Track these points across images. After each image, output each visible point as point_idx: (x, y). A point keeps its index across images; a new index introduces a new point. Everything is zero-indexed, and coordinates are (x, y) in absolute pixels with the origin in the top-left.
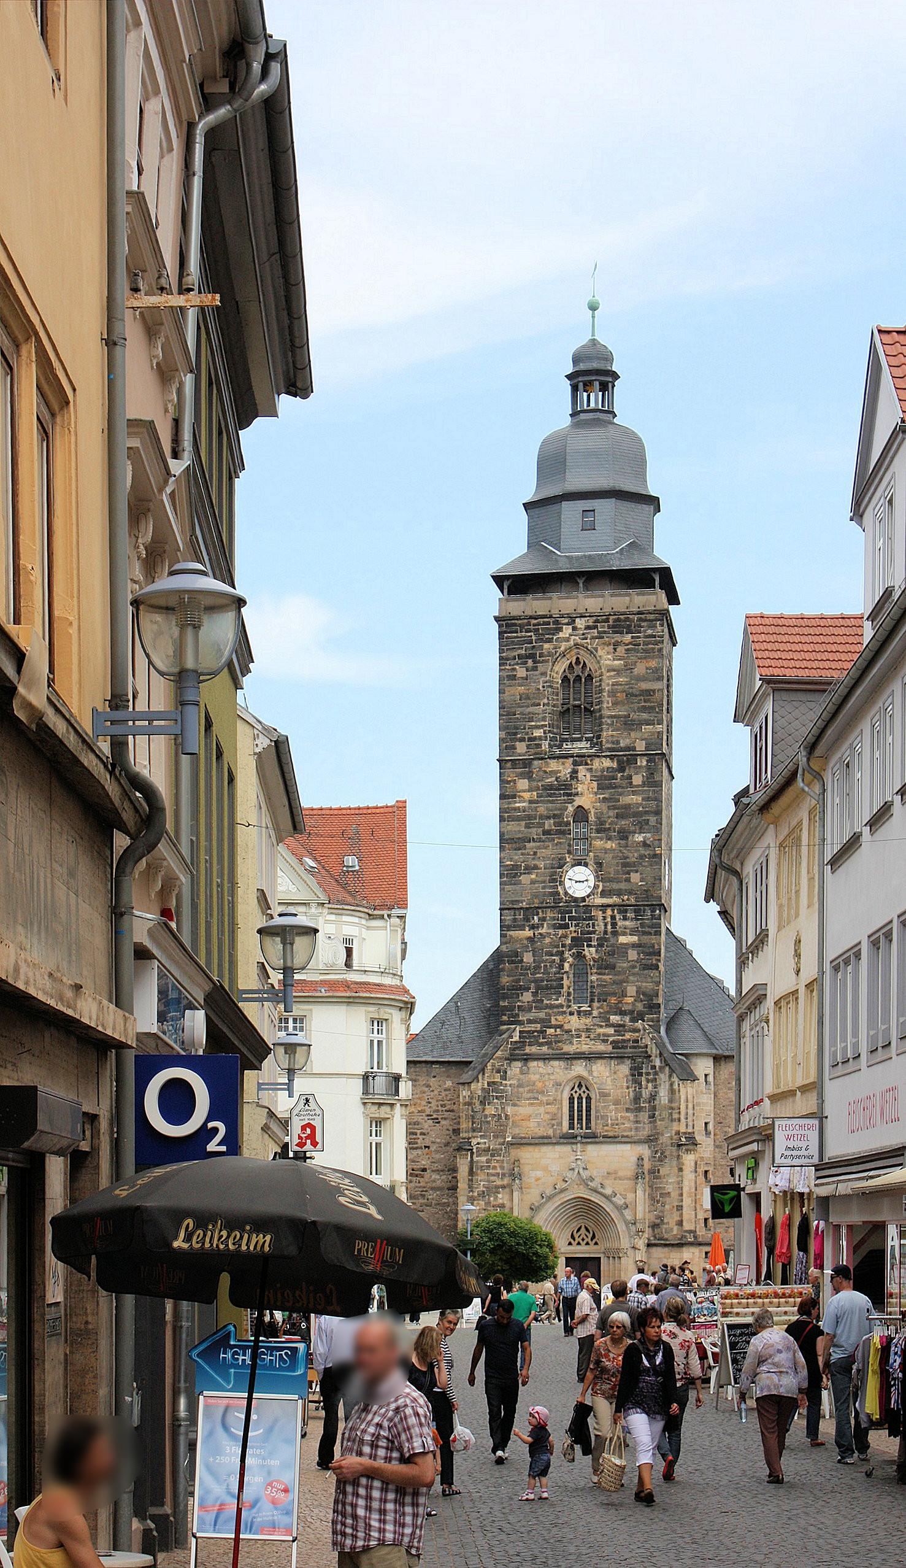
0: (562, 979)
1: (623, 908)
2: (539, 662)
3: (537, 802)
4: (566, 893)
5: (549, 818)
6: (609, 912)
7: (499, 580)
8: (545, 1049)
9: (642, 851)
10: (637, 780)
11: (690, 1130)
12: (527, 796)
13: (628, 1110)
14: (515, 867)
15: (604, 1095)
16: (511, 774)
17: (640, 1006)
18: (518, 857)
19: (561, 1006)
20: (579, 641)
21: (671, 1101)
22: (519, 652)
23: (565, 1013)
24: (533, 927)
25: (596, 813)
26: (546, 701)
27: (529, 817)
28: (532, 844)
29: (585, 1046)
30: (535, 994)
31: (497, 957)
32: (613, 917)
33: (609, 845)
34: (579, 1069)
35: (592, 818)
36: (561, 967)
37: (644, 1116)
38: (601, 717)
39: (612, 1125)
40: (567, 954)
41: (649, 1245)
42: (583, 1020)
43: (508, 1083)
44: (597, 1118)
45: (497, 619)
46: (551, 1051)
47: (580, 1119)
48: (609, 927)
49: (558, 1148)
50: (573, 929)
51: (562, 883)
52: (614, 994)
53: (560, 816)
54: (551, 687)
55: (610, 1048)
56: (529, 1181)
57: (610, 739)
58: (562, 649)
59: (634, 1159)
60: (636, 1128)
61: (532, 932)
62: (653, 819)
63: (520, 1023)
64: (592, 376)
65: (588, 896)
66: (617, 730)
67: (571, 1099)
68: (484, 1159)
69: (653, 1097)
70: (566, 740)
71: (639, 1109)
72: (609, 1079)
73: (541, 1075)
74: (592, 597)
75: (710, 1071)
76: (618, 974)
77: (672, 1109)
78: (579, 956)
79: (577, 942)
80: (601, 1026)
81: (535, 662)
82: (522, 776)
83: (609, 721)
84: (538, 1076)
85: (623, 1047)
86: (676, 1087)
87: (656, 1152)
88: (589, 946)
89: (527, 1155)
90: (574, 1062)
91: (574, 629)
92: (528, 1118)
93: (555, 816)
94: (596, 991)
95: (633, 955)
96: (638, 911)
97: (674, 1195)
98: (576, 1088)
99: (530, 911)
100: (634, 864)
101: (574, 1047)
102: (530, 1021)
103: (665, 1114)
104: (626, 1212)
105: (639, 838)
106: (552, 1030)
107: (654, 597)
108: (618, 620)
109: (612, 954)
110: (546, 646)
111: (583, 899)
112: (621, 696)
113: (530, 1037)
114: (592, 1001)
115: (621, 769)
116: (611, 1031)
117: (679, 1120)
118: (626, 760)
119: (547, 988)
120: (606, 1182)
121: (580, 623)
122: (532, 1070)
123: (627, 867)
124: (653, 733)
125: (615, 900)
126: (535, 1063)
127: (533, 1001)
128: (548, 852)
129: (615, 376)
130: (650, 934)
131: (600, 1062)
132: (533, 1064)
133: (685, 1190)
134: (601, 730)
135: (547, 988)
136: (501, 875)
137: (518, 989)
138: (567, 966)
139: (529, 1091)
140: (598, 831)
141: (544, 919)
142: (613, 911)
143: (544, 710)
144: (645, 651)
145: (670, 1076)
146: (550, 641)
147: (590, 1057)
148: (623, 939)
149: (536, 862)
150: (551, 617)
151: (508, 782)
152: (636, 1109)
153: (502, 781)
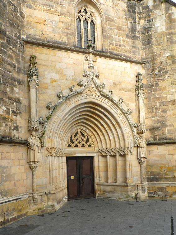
44: (103, 37)
56: (45, 81)
92: (44, 22)
98: (82, 13)
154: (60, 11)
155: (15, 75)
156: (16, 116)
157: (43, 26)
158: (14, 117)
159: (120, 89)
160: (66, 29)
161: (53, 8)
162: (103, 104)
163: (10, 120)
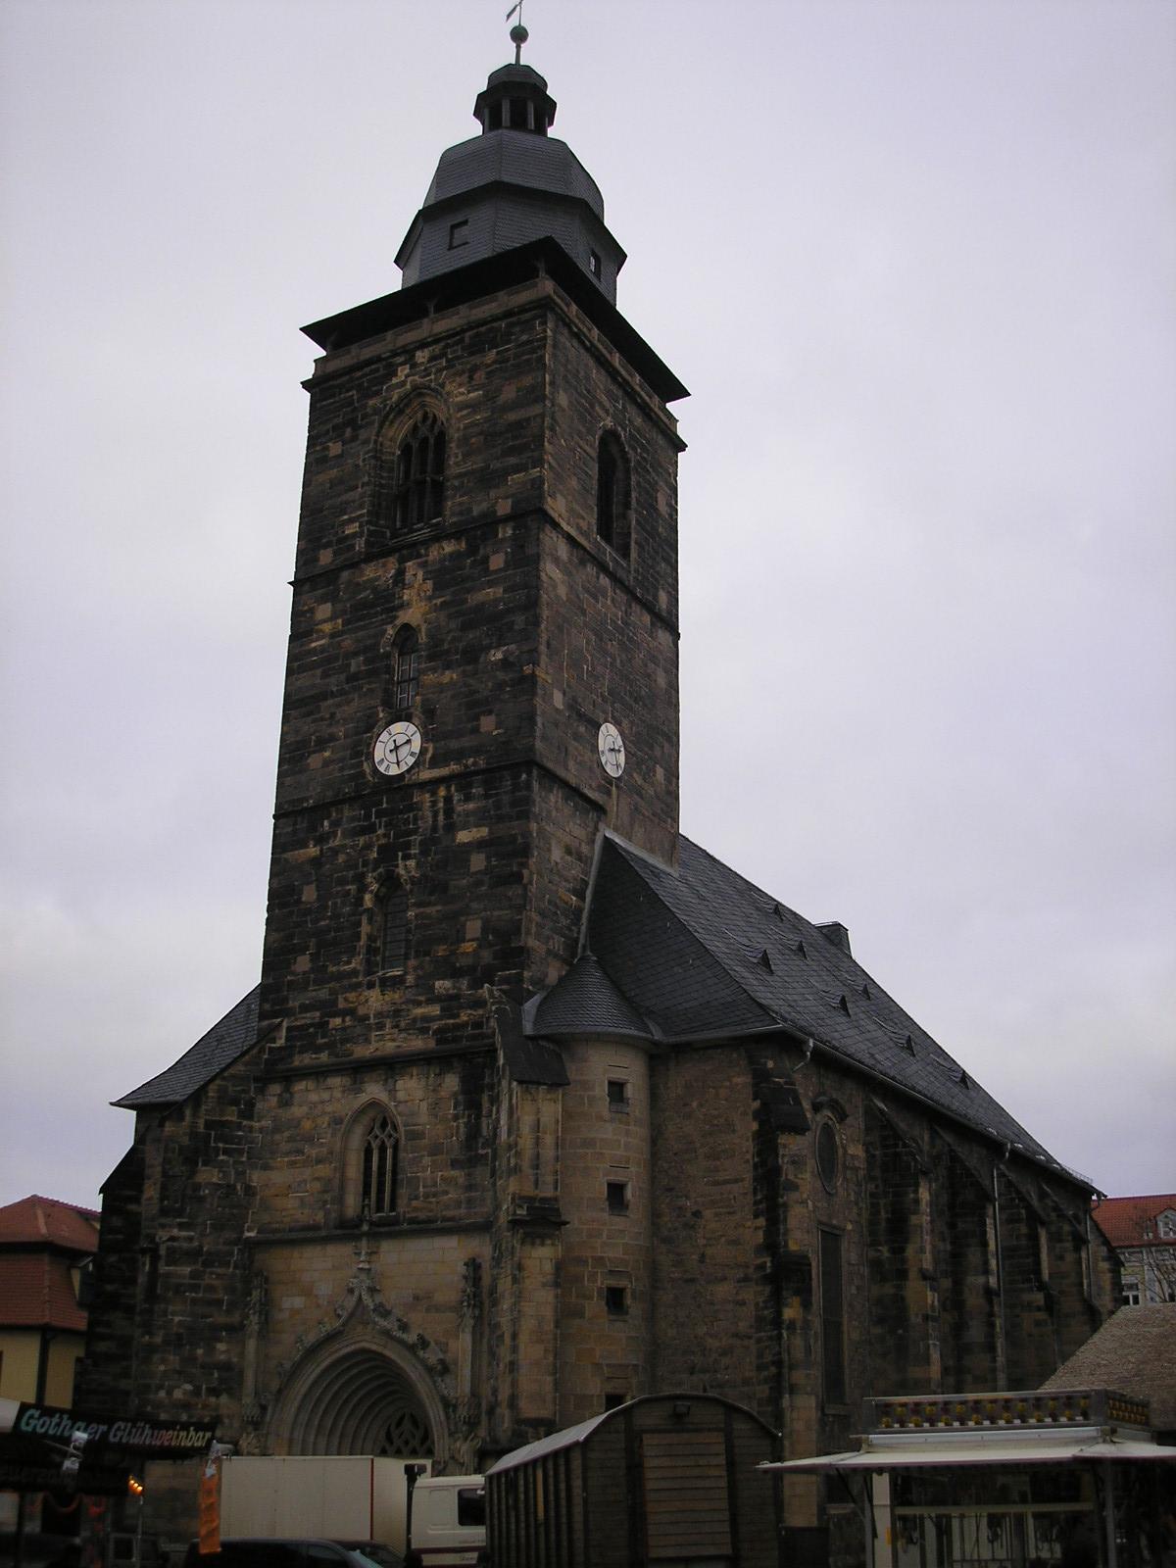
0: (359, 924)
2: (361, 427)
3: (342, 633)
4: (375, 771)
5: (356, 654)
6: (442, 792)
7: (315, 331)
8: (324, 1057)
9: (501, 675)
10: (497, 562)
15: (415, 1136)
19: (354, 973)
22: (336, 421)
24: (321, 840)
25: (428, 630)
26: (366, 479)
29: (387, 1043)
30: (314, 957)
32: (448, 800)
33: (449, 676)
34: (374, 1090)
35: (423, 638)
36: (360, 901)
39: (427, 1196)
43: (257, 1125)
45: (306, 385)
48: (441, 817)
49: (331, 1249)
50: (380, 832)
51: (370, 756)
53: (375, 646)
54: (374, 457)
55: (432, 1044)
58: (395, 398)
59: (462, 1269)
61: (318, 848)
62: (520, 620)
65: (408, 771)
67: (368, 1152)
78: (390, 881)
79: (388, 854)
80: (419, 1004)
81: (354, 430)
82: (323, 600)
84: (305, 1109)
85: (455, 1040)
88: (406, 857)
91: (413, 366)
95: (478, 862)
101: (372, 1048)
102: (305, 1008)
106: (338, 1021)
108: (477, 335)
114: (406, 957)
116: (435, 1010)
118: (479, 531)
121: (421, 356)
122: (297, 1098)
123: (476, 706)
132: (299, 1086)
139: (291, 1139)
140: (431, 658)
141: (335, 824)
142: (448, 789)
146: (378, 393)
147: (391, 1067)
148: (463, 836)
149: (334, 730)
151: (304, 613)
154: (314, 1156)
155: (222, 1319)
156: (218, 1396)
158: (213, 1399)
159: (428, 1310)
160: (325, 1192)
161: (303, 1153)
163: (200, 1406)
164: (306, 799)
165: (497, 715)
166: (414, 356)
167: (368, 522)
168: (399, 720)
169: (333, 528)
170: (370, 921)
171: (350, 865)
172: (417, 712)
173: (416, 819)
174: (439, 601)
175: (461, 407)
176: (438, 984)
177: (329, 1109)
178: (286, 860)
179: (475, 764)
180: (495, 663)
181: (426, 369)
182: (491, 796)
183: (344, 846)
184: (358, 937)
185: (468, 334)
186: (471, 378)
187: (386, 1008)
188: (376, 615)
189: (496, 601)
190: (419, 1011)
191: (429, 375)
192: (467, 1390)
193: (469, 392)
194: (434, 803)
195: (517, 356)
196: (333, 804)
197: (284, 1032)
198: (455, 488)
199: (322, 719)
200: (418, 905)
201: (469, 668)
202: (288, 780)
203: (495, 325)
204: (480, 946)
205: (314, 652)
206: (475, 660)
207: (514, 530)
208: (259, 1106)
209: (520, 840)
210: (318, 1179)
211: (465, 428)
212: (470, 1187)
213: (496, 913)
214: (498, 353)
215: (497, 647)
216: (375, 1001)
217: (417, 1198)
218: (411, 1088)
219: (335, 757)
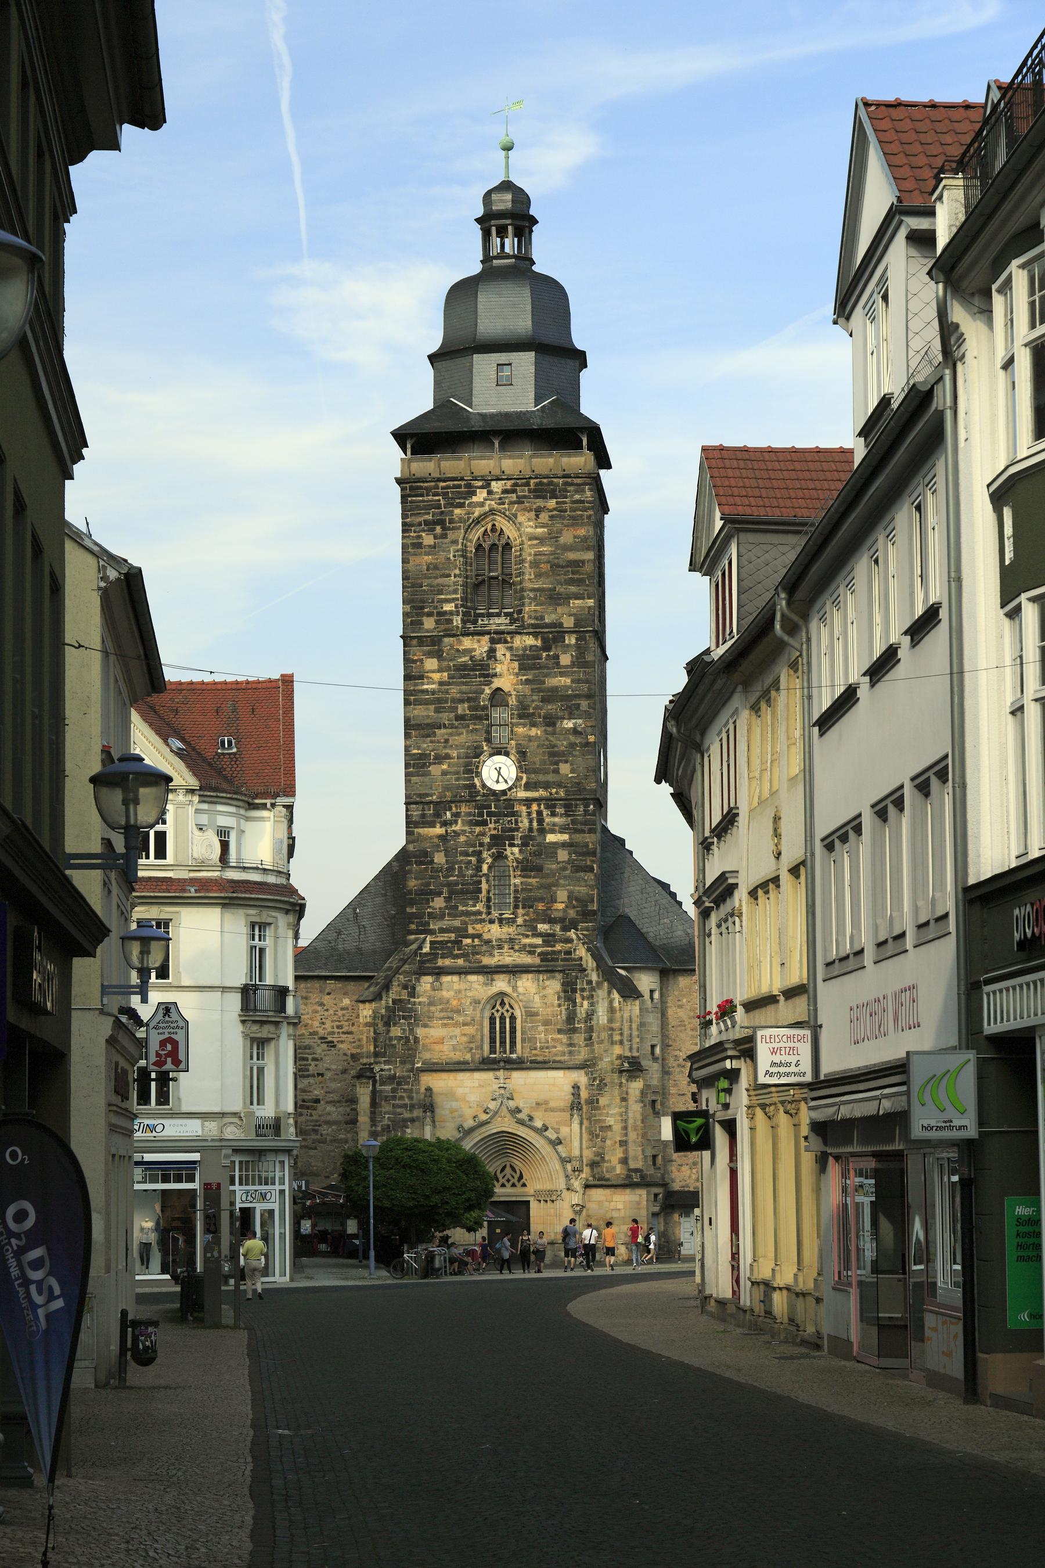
0: (480, 882)
1: (550, 803)
2: (449, 529)
3: (449, 684)
4: (484, 786)
5: (462, 701)
6: (535, 807)
8: (460, 962)
9: (572, 738)
10: (565, 660)
11: (635, 1054)
12: (436, 677)
13: (560, 1031)
14: (423, 756)
15: (530, 1014)
16: (417, 654)
17: (572, 913)
18: (426, 745)
19: (479, 913)
20: (496, 506)
21: (611, 1020)
22: (427, 517)
23: (483, 921)
24: (444, 824)
26: (457, 572)
27: (439, 701)
28: (443, 731)
29: (508, 958)
30: (448, 899)
31: (402, 856)
32: (539, 813)
33: (534, 731)
34: (501, 984)
35: (513, 701)
36: (479, 868)
37: (579, 1039)
38: (522, 590)
39: (542, 1048)
40: (485, 855)
41: (587, 1186)
42: (505, 929)
43: (417, 1000)
44: (523, 1040)
46: (467, 964)
47: (503, 1042)
48: (535, 824)
49: (477, 1075)
50: (492, 826)
51: (479, 774)
52: (541, 899)
53: (476, 699)
54: (462, 556)
55: (537, 961)
56: (443, 1113)
57: (533, 614)
58: (476, 514)
59: (568, 1089)
60: (570, 1053)
63: (431, 932)
64: (509, 217)
65: (510, 789)
66: (541, 605)
68: (388, 1088)
69: (590, 1016)
70: (482, 615)
71: (574, 1030)
72: (536, 995)
73: (459, 991)
74: (510, 457)
75: (656, 986)
76: (546, 876)
77: (612, 1029)
79: (498, 841)
80: (527, 936)
81: (444, 529)
82: (430, 654)
83: (532, 595)
84: (452, 993)
85: (553, 960)
86: (616, 1004)
87: (594, 1079)
88: (512, 845)
89: (439, 1082)
90: (496, 977)
91: (490, 493)
92: (441, 1041)
93: (469, 700)
94: (521, 896)
95: (563, 855)
96: (569, 809)
97: (617, 1128)
99: (441, 806)
100: (562, 754)
102: (442, 931)
103: (604, 1035)
104: (560, 1148)
105: (569, 724)
106: (469, 941)
107: (583, 459)
108: (541, 484)
109: (538, 854)
110: (457, 511)
111: (504, 792)
112: (545, 567)
113: (442, 949)
114: (516, 907)
115: (546, 648)
116: (539, 941)
117: (621, 1042)
118: (552, 636)
119: (462, 892)
120: (535, 1114)
122: (445, 986)
123: (556, 756)
124: (582, 608)
125: (541, 793)
126: (448, 978)
127: (446, 907)
128: (463, 738)
129: (534, 221)
130: (582, 831)
131: (525, 976)
132: (446, 979)
133: (630, 1122)
134: (523, 605)
135: (462, 892)
136: (407, 766)
137: (427, 894)
138: (485, 867)
139: (442, 1011)
140: (520, 717)
141: (457, 815)
142: (539, 805)
143: (454, 579)
144: (573, 518)
145: (609, 993)
146: (461, 505)
147: (514, 971)
148: (551, 838)
150: (462, 479)
152: (570, 1030)
153: (407, 660)
157: (441, 1046)
159: (546, 1111)
162: (519, 1133)
164: (427, 795)
165: (572, 764)
166: (489, 485)
167: (462, 606)
168: (499, 753)
169: (433, 602)
170: (488, 881)
171: (468, 844)
172: (513, 751)
173: (516, 822)
174: (524, 678)
175: (532, 538)
176: (540, 926)
177: (469, 994)
178: (419, 834)
179: (557, 793)
180: (568, 730)
181: (500, 499)
182: (569, 816)
183: (464, 831)
184: (480, 891)
185: (532, 481)
186: (537, 516)
187: (503, 937)
188: (476, 676)
189: (567, 687)
190: (527, 941)
191: (504, 504)
192: (576, 1152)
193: (536, 527)
194: (529, 814)
195: (573, 510)
196: (452, 802)
197: (428, 945)
198: (530, 598)
199: (439, 742)
200: (523, 877)
201: (548, 729)
202: (414, 779)
203: (555, 480)
204: (567, 907)
205: (426, 691)
206: (554, 724)
207: (577, 639)
208: (418, 989)
209: (591, 846)
210: (465, 1035)
211: (535, 555)
212: (571, 1045)
213: (577, 888)
214: (557, 503)
215: (570, 719)
216: (495, 932)
217: (535, 1049)
218: (526, 984)
219: (452, 770)
